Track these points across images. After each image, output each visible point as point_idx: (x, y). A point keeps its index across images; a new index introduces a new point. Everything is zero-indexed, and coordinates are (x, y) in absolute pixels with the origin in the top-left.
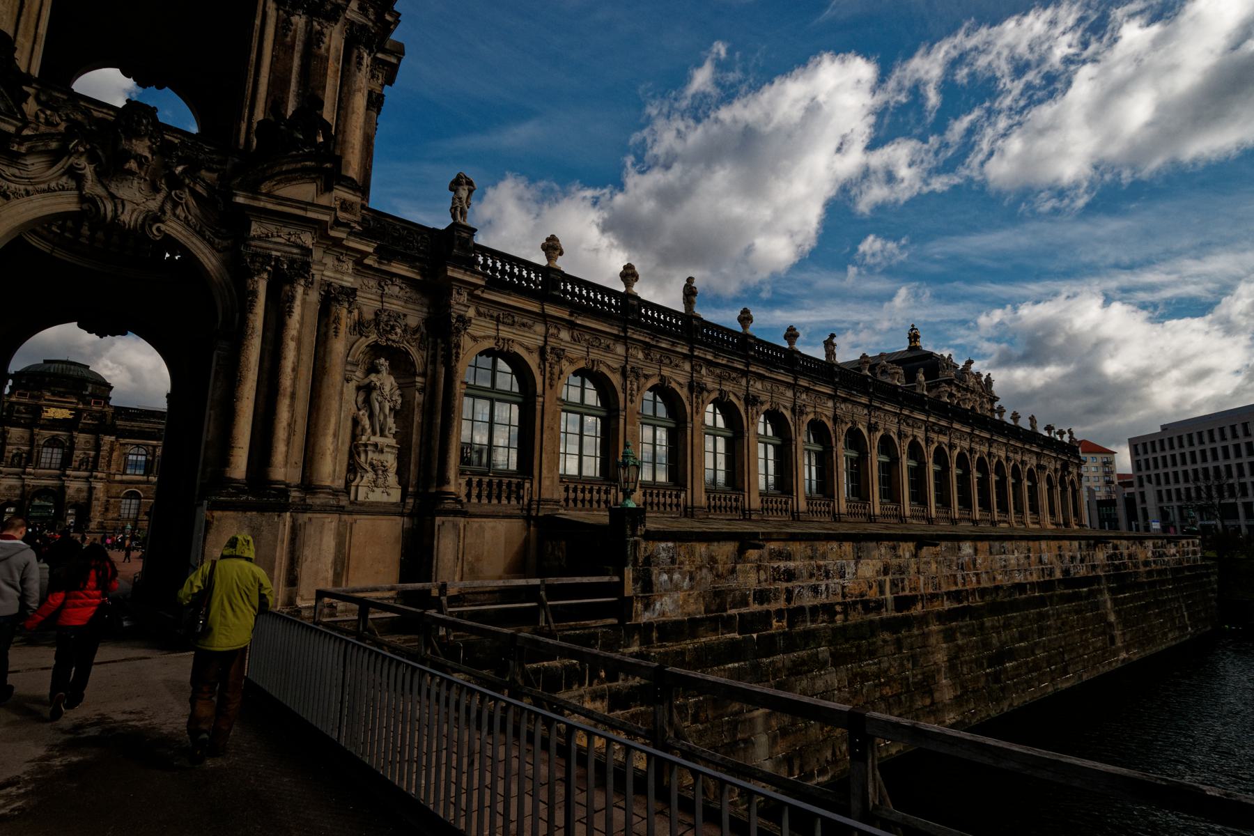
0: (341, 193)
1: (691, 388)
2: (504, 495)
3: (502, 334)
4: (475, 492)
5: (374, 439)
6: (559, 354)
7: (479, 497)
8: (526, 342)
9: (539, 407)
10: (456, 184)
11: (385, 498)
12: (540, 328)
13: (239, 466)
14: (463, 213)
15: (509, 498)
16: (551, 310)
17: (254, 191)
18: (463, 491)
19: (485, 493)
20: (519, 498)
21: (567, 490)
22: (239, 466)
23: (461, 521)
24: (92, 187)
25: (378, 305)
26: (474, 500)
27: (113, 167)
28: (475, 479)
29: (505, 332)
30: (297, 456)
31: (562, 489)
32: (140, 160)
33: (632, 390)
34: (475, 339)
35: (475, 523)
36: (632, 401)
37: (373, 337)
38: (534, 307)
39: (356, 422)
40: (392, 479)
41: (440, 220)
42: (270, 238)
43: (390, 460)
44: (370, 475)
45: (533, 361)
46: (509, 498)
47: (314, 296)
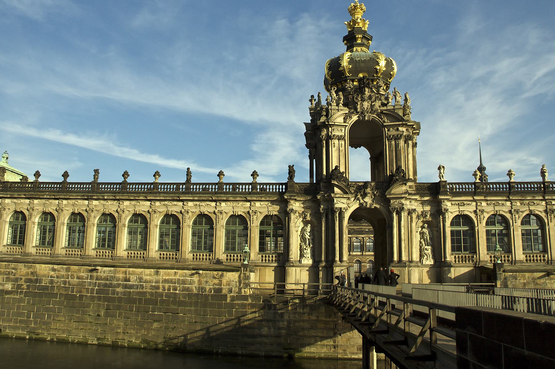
0: (409, 184)
2: (467, 261)
4: (457, 260)
5: (426, 247)
6: (482, 211)
7: (459, 261)
8: (470, 210)
9: (476, 231)
10: (439, 168)
12: (474, 203)
15: (469, 261)
16: (476, 198)
19: (460, 260)
20: (473, 261)
22: (396, 258)
24: (362, 201)
25: (422, 210)
26: (457, 262)
27: (364, 195)
28: (457, 256)
29: (462, 208)
30: (407, 254)
32: (369, 193)
33: (515, 218)
34: (451, 213)
37: (422, 219)
38: (470, 198)
39: (420, 242)
42: (394, 203)
44: (426, 257)
45: (473, 216)
46: (469, 261)
47: (406, 214)
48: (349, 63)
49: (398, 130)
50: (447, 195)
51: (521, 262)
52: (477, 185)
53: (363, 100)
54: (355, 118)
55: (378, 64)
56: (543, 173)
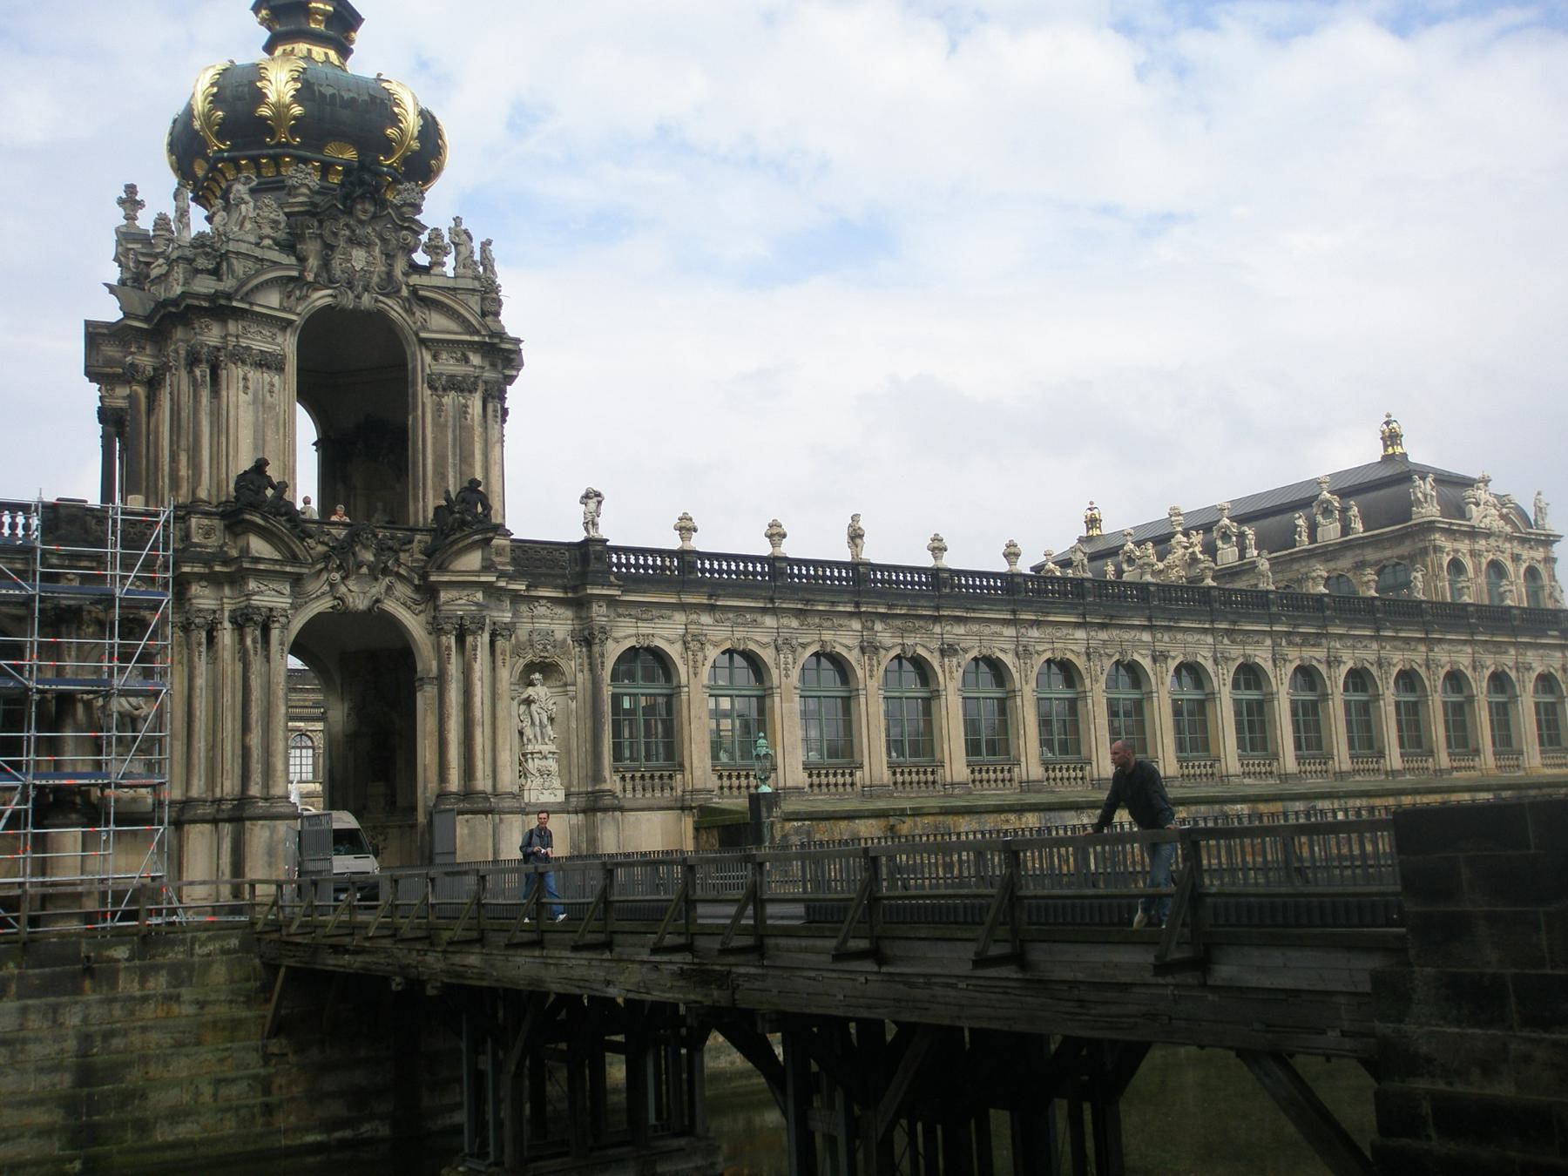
1: (863, 650)
3: (641, 631)
5: (538, 748)
8: (665, 633)
10: (586, 497)
11: (552, 799)
12: (680, 617)
13: (454, 783)
14: (595, 524)
17: (442, 568)
18: (618, 787)
21: (720, 777)
23: (618, 814)
26: (629, 795)
28: (628, 775)
29: (645, 628)
31: (715, 778)
33: (786, 663)
35: (631, 816)
36: (787, 676)
39: (521, 733)
40: (557, 783)
41: (578, 536)
43: (552, 764)
45: (674, 651)
48: (298, 97)
49: (466, 360)
50: (611, 585)
51: (798, 790)
52: (688, 558)
53: (354, 241)
54: (321, 298)
55: (395, 120)
56: (855, 536)
